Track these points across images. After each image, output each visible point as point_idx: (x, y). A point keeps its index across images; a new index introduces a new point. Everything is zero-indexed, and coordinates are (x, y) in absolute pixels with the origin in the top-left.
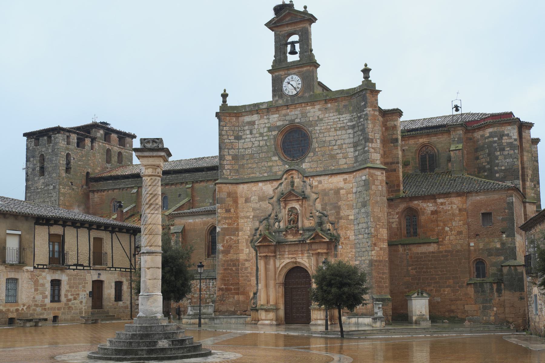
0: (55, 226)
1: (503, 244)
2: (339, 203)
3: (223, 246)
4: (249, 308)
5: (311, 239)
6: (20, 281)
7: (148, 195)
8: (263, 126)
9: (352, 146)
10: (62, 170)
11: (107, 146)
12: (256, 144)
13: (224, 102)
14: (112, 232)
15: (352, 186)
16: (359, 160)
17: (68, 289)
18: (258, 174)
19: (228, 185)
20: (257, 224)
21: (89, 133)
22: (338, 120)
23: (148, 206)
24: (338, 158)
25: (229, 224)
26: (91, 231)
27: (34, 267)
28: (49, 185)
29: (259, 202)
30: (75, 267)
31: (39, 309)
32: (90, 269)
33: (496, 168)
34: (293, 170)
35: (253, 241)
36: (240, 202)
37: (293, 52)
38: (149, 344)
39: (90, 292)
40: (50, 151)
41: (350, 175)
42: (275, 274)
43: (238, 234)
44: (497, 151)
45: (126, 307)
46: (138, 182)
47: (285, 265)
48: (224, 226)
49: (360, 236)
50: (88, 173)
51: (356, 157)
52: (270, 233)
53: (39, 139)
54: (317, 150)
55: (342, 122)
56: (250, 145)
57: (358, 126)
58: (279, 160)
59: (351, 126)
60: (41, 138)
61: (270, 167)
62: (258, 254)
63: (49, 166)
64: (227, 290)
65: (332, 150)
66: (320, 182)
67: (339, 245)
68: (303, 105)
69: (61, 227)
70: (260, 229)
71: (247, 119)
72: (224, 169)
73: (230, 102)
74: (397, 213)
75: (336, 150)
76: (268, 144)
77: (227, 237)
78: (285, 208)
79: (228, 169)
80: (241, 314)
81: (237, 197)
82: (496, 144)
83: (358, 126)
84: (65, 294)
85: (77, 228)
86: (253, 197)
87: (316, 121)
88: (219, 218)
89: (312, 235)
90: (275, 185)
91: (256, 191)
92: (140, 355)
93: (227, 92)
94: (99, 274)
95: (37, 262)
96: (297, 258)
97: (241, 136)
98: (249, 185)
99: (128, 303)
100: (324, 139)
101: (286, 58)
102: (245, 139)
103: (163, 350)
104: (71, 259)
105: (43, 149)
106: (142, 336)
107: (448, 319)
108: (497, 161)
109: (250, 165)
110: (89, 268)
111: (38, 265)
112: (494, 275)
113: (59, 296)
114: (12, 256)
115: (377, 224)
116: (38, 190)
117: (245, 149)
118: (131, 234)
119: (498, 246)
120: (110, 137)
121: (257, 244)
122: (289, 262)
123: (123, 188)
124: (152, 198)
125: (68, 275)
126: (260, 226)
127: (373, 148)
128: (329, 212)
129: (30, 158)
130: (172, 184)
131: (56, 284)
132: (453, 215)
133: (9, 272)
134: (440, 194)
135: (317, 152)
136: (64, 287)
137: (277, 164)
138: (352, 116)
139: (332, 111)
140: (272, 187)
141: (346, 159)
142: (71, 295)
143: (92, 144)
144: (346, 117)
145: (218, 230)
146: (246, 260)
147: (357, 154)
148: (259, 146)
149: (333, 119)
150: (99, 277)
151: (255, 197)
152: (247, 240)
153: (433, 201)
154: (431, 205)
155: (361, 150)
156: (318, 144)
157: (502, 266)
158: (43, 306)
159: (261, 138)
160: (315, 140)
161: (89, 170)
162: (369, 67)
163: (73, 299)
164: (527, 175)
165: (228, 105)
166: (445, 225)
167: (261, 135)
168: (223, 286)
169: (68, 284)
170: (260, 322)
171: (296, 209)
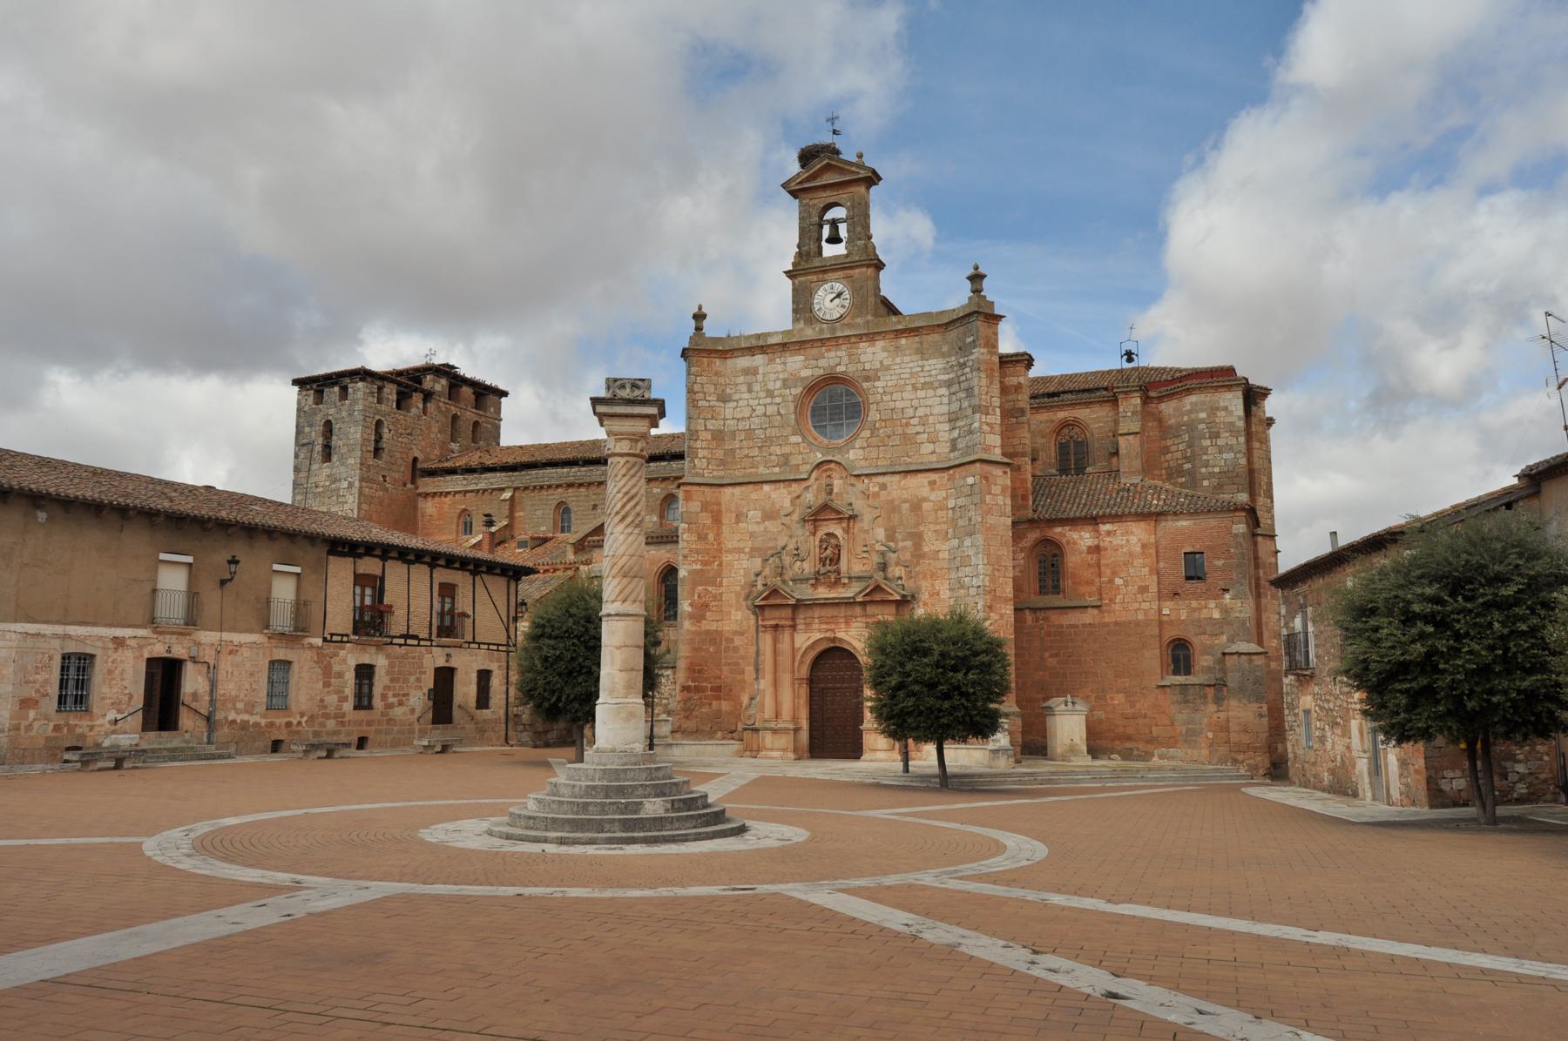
0: (366, 558)
1: (1226, 611)
2: (921, 528)
3: (691, 605)
4: (740, 728)
6: (295, 667)
7: (620, 495)
8: (772, 377)
10: (368, 451)
11: (454, 410)
12: (760, 411)
13: (699, 329)
14: (474, 573)
16: (960, 446)
17: (388, 683)
18: (762, 470)
19: (703, 488)
20: (758, 562)
21: (420, 383)
22: (919, 369)
23: (619, 517)
25: (705, 563)
26: (434, 571)
27: (325, 640)
28: (340, 480)
29: (763, 521)
30: (402, 641)
31: (331, 724)
32: (432, 645)
33: (1203, 470)
34: (830, 461)
35: (751, 597)
36: (725, 520)
37: (834, 239)
38: (626, 808)
39: (430, 690)
40: (344, 414)
43: (721, 582)
44: (1205, 438)
45: (496, 721)
46: (513, 479)
47: (813, 643)
48: (695, 567)
49: (962, 591)
50: (415, 460)
51: (954, 442)
52: (784, 582)
53: (322, 392)
54: (877, 425)
55: (927, 374)
56: (747, 413)
57: (959, 383)
58: (803, 442)
59: (945, 381)
60: (326, 390)
61: (786, 457)
62: (760, 623)
63: (341, 443)
64: (698, 689)
65: (907, 425)
66: (883, 487)
68: (853, 340)
69: (377, 560)
70: (764, 574)
71: (744, 362)
72: (696, 457)
73: (711, 329)
74: (1022, 550)
76: (782, 412)
77: (700, 588)
78: (814, 534)
79: (704, 458)
80: (724, 738)
81: (720, 511)
82: (1202, 426)
83: (959, 383)
84: (382, 694)
85: (410, 563)
86: (752, 512)
87: (877, 370)
88: (686, 551)
89: (868, 586)
92: (609, 831)
93: (704, 310)
94: (448, 655)
95: (331, 628)
97: (730, 395)
98: (743, 488)
99: (502, 712)
100: (892, 405)
101: (820, 248)
102: (737, 401)
103: (658, 822)
104: (397, 625)
105: (332, 411)
106: (608, 792)
107: (1119, 753)
108: (1205, 457)
109: (746, 452)
110: (429, 643)
111: (332, 635)
112: (1209, 669)
113: (370, 697)
114: (282, 619)
115: (994, 569)
116: (318, 490)
117: (738, 420)
118: (510, 578)
119: (1216, 615)
120: (458, 393)
121: (758, 602)
122: (821, 639)
123: (485, 491)
124: (629, 501)
125: (388, 656)
126: (764, 567)
127: (988, 424)
129: (303, 427)
130: (581, 485)
131: (365, 673)
132: (1131, 555)
133: (276, 647)
134: (1104, 516)
136: (380, 681)
138: (948, 362)
139: (908, 352)
140: (789, 493)
141: (934, 443)
142: (394, 696)
143: (424, 403)
144: (935, 366)
145: (682, 573)
146: (736, 633)
147: (956, 436)
148: (765, 415)
149: (911, 368)
150: (447, 661)
152: (738, 594)
153: (1090, 528)
154: (1087, 535)
155: (964, 426)
157: (1224, 654)
158: (339, 716)
159: (769, 400)
160: (873, 407)
161: (417, 454)
162: (982, 270)
163: (396, 704)
164: (1260, 484)
165: (707, 335)
166: (1114, 573)
167: (770, 394)
168: (690, 683)
169: (388, 673)
170: (763, 753)
171: (836, 537)
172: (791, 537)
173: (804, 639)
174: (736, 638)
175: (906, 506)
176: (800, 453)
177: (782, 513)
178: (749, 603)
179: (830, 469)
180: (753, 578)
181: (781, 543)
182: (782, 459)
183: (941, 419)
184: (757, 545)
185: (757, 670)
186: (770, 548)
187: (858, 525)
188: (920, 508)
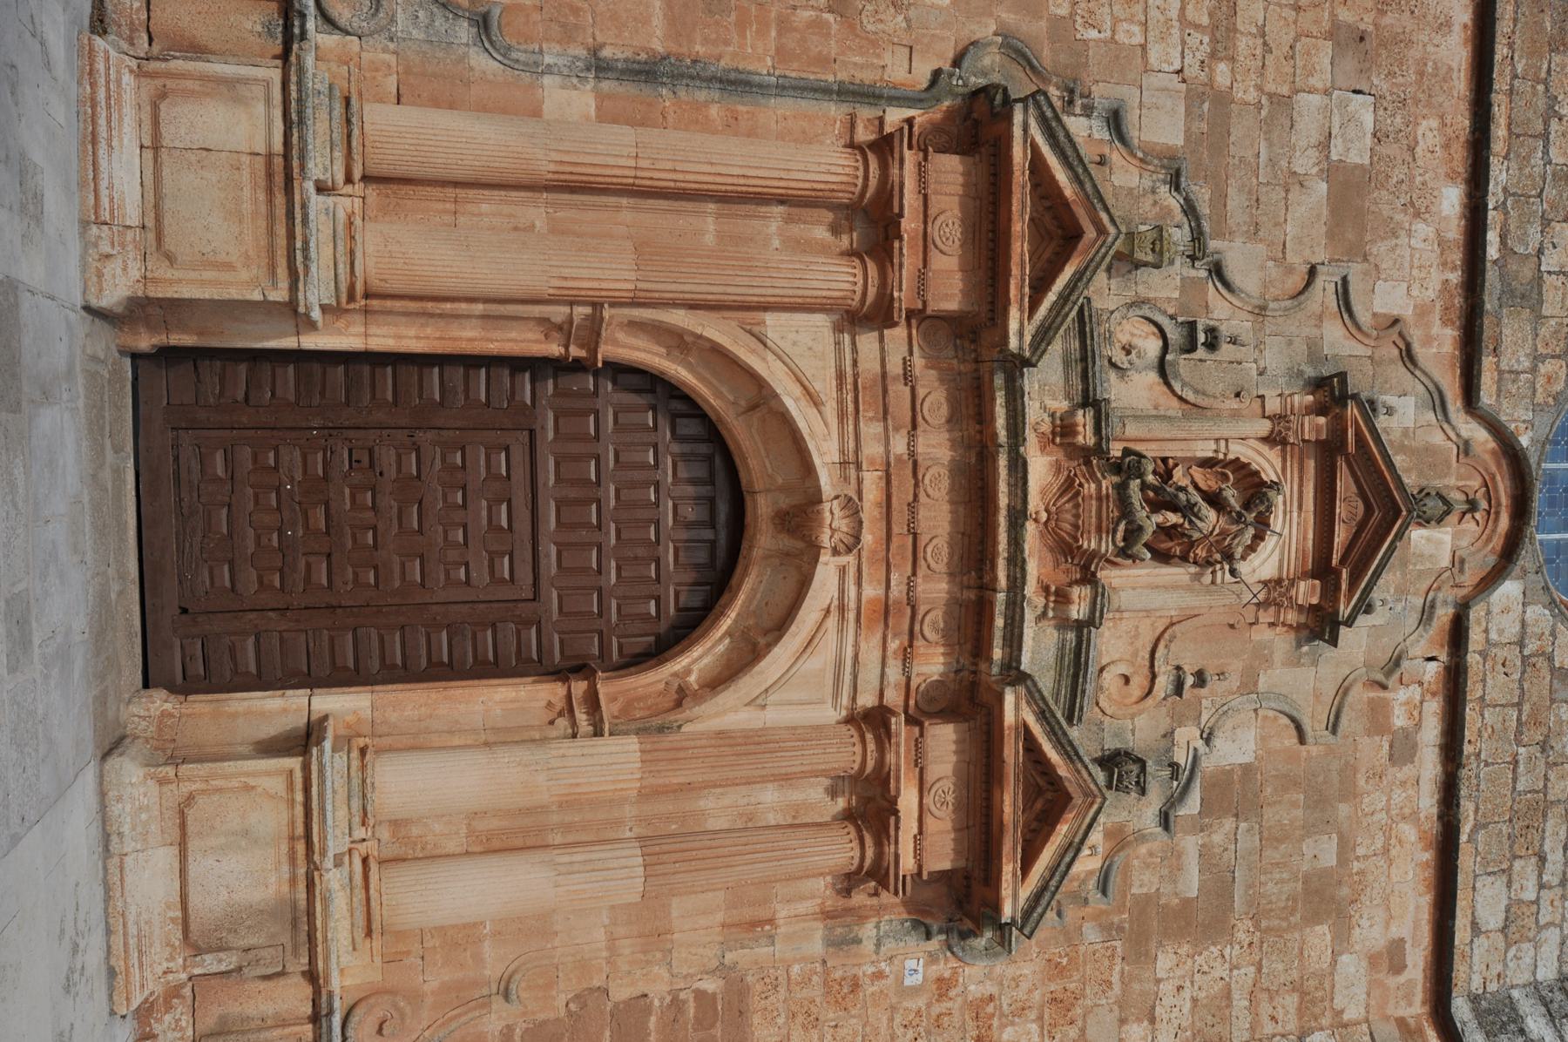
5: (1031, 746)
15: (1346, 1017)
24: (1518, 864)
29: (1333, 171)
41: (1419, 995)
42: (693, 306)
47: (785, 419)
66: (1402, 750)
67: (932, 959)
70: (1116, 157)
86: (1368, 119)
90: (1428, 341)
91: (1412, 149)
96: (849, 560)
98: (1461, 84)
121: (1024, 131)
122: (808, 469)
126: (1145, 157)
128: (1190, 844)
140: (1422, 312)
141: (1504, 930)
151: (1369, 140)
172: (1261, 311)
173: (808, 367)
176: (1537, 358)
177: (1355, 271)
178: (990, 67)
179: (1492, 514)
180: (1103, 94)
181: (1238, 256)
182: (1527, 272)
184: (1236, 133)
185: (646, 72)
186: (1220, 198)
187: (1280, 642)
188: (1314, 918)
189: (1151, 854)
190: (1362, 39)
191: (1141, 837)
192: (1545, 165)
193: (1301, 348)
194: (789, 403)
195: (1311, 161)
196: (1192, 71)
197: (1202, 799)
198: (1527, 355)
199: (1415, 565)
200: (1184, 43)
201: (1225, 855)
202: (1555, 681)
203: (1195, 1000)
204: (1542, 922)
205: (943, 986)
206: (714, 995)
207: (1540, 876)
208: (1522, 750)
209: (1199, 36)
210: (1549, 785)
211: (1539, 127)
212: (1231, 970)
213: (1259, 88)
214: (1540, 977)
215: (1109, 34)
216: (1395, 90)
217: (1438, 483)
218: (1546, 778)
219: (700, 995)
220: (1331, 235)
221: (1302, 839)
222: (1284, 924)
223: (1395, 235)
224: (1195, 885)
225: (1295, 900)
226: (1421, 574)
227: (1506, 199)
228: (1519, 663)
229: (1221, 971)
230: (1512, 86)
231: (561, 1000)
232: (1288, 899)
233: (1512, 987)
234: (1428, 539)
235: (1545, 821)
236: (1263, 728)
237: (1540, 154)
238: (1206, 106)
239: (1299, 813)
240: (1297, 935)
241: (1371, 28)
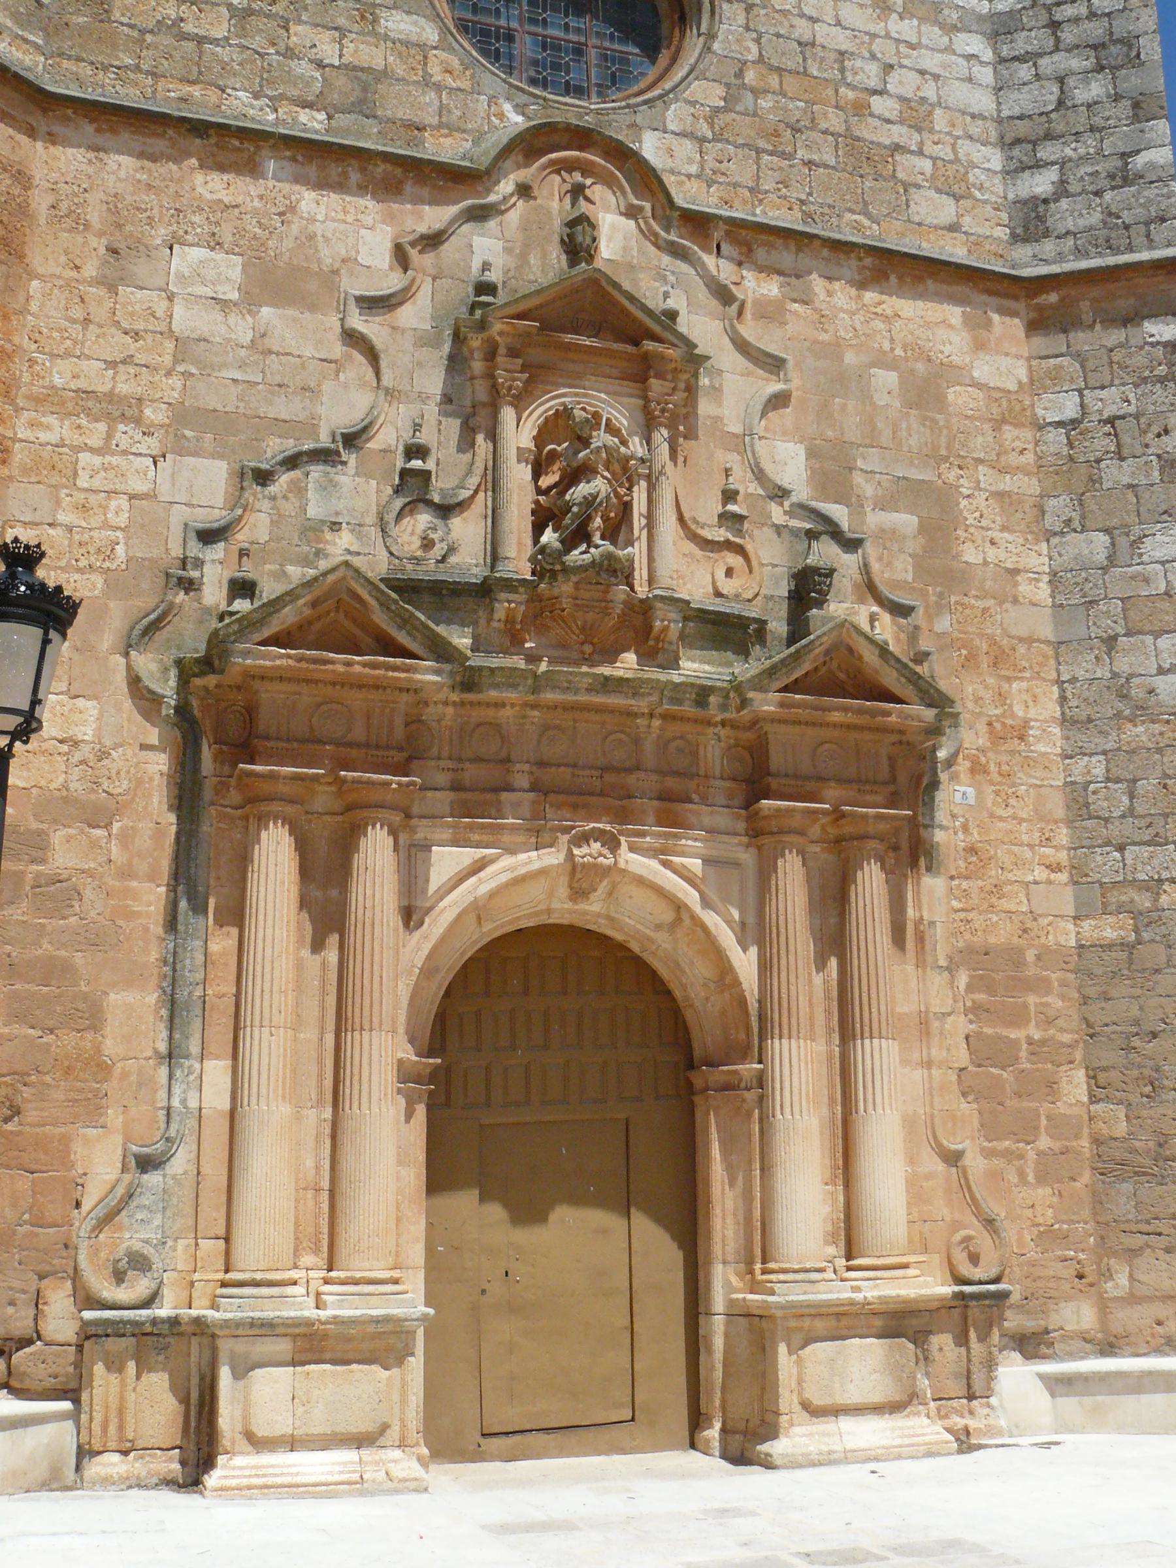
9: (994, 136)
15: (1025, 380)
29: (250, 301)
54: (750, 76)
57: (1054, 25)
70: (241, 537)
75: (888, 121)
83: (1054, 25)
86: (197, 254)
128: (875, 519)
135: (756, 92)
137: (427, 76)
141: (957, 198)
151: (219, 256)
156: (758, 41)
174: (58, 837)
175: (886, 380)
176: (426, 82)
182: (341, 81)
183: (976, 129)
184: (213, 403)
186: (280, 425)
188: (940, 401)
189: (880, 559)
190: (115, 252)
191: (865, 568)
192: (230, 45)
193: (425, 353)
194: (484, 889)
195: (240, 322)
196: (152, 444)
197: (836, 502)
198: (424, 93)
199: (633, 257)
200: (125, 453)
201: (884, 484)
202: (738, 108)
203: (1004, 528)
204: (952, 157)
205: (977, 769)
206: (971, 977)
207: (912, 152)
208: (800, 153)
209: (118, 435)
210: (831, 129)
211: (190, 46)
212: (980, 490)
213: (168, 374)
214: (999, 168)
215: (119, 534)
216: (167, 220)
217: (557, 223)
218: (825, 132)
219: (970, 988)
220: (313, 308)
221: (873, 404)
222: (945, 431)
223: (312, 237)
224: (908, 516)
225: (925, 418)
226: (641, 251)
227: (267, 96)
228: (720, 145)
229: (980, 499)
230: (148, 73)
231: (964, 1106)
232: (924, 425)
233: (1005, 198)
234: (610, 239)
235: (865, 140)
236: (775, 432)
237: (218, 49)
238: (188, 433)
239: (851, 404)
240: (954, 420)
241: (104, 241)
